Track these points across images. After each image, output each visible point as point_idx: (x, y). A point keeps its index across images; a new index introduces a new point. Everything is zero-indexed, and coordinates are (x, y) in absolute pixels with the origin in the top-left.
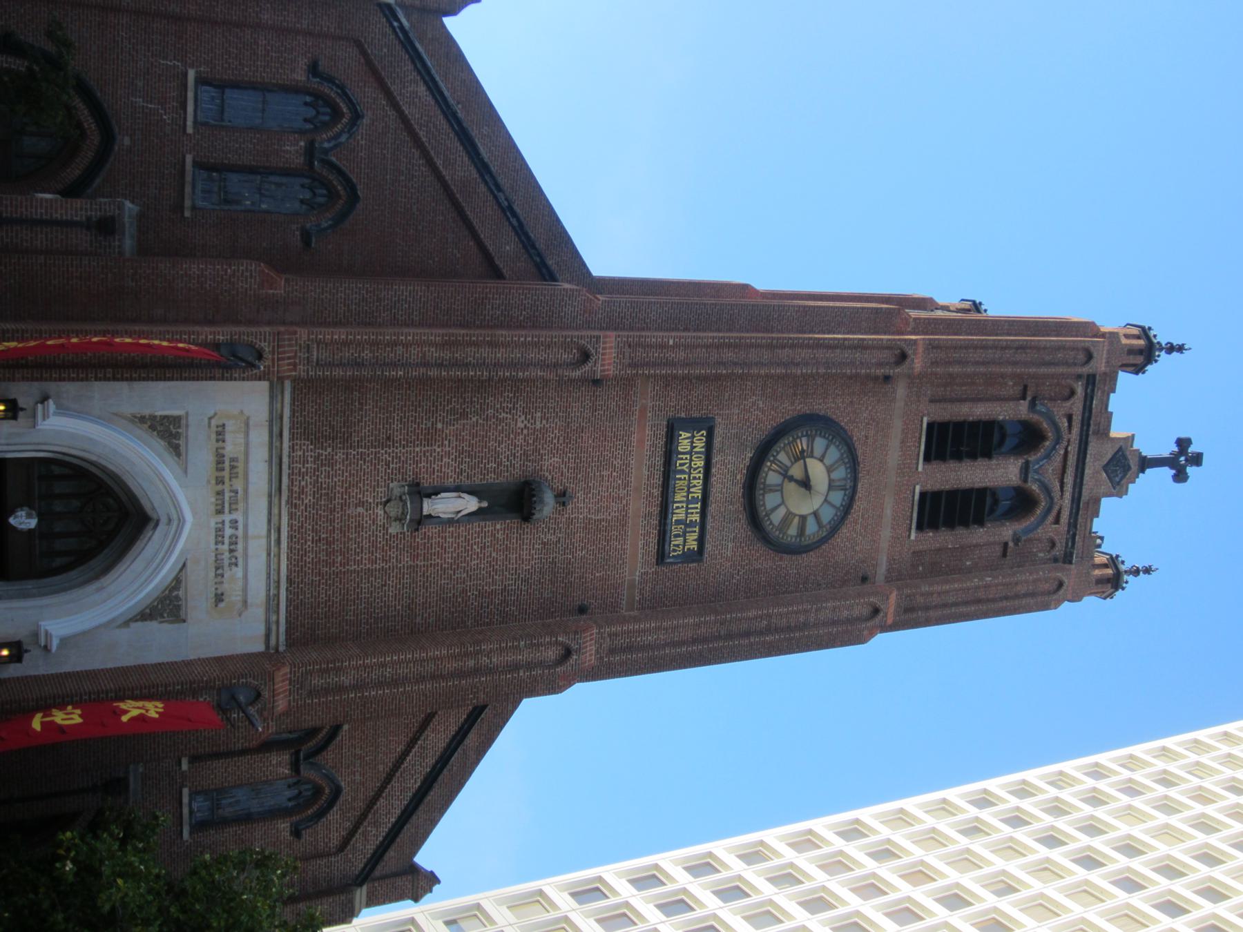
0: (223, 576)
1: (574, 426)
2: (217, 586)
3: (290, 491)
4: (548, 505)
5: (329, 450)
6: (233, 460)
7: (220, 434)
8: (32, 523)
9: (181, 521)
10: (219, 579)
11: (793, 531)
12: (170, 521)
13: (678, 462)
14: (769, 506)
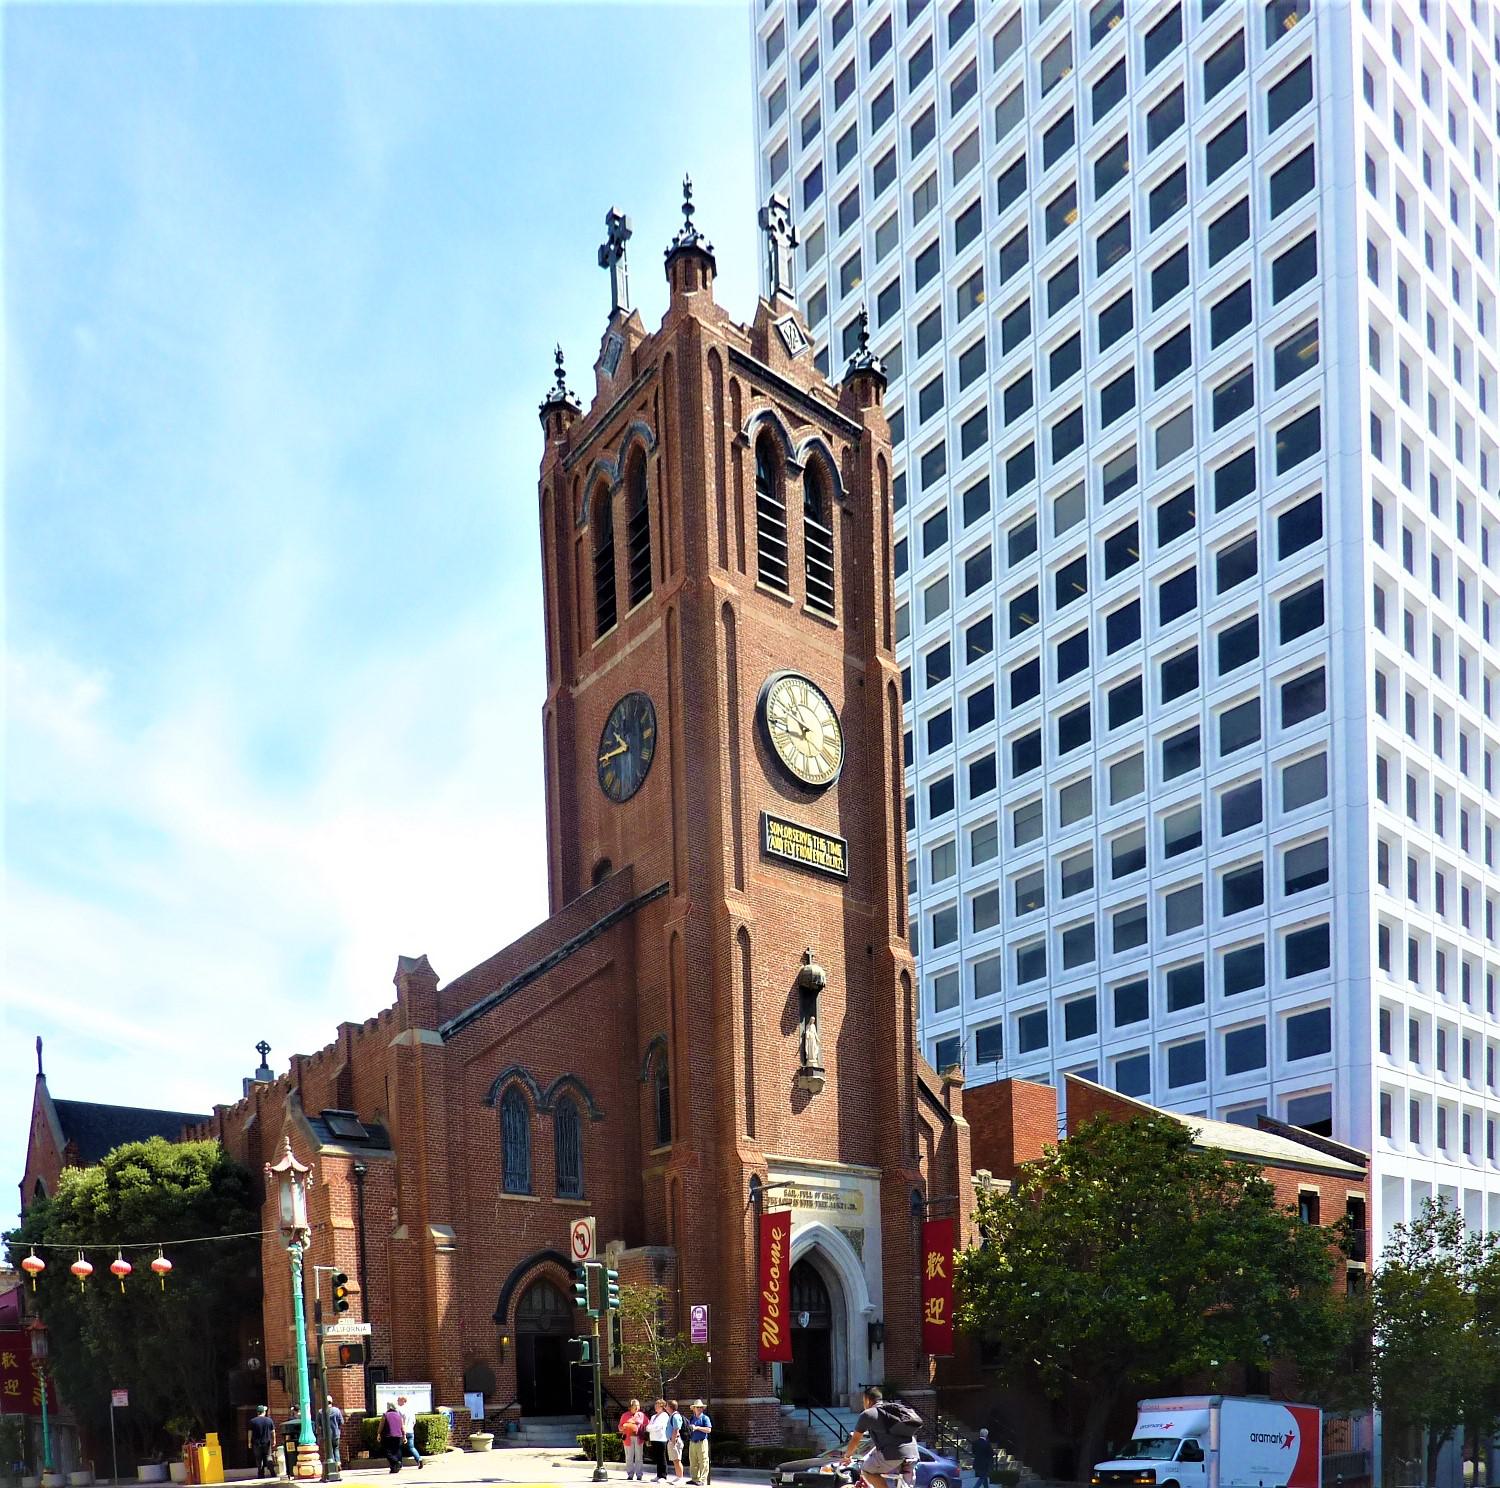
4: (815, 968)
9: (818, 1228)
12: (816, 1235)
14: (817, 772)
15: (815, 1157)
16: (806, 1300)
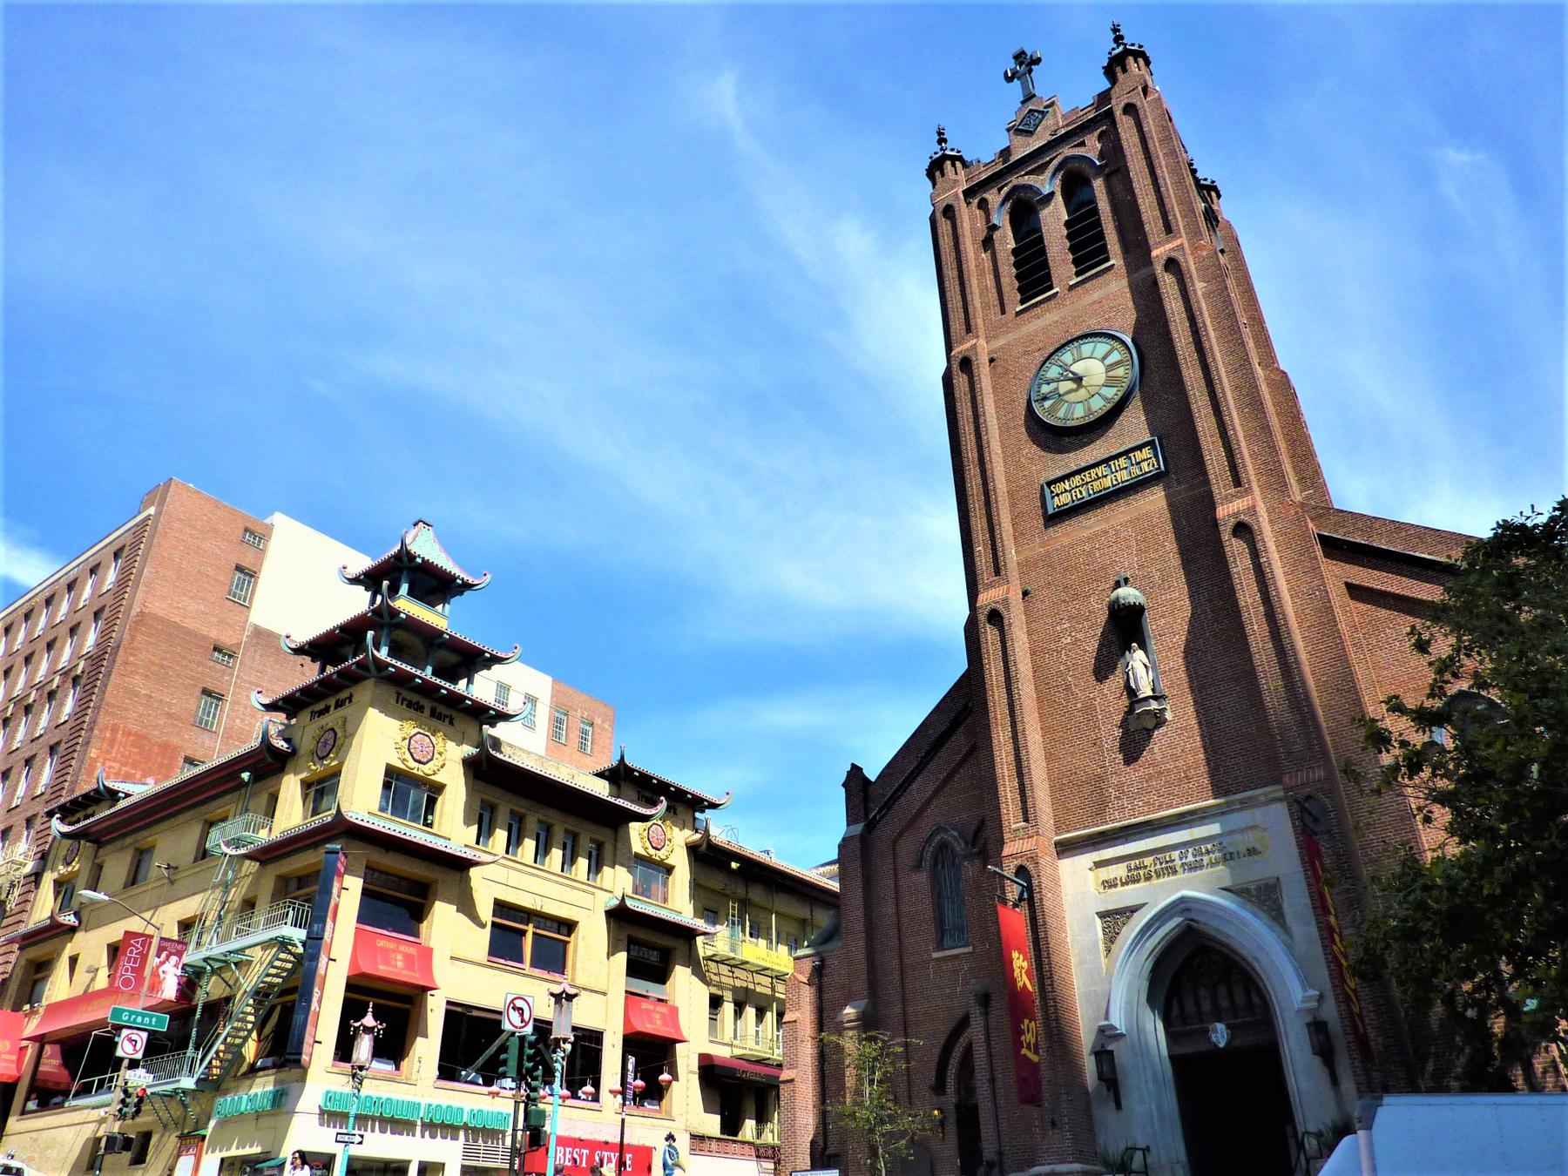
0: (1231, 853)
1: (1063, 596)
2: (1241, 855)
3: (1148, 813)
4: (1129, 594)
5: (1111, 790)
6: (1130, 871)
7: (1109, 884)
8: (1220, 1027)
9: (1182, 900)
10: (1235, 856)
11: (1120, 372)
13: (1079, 496)
15: (1168, 808)
16: (1225, 1004)
